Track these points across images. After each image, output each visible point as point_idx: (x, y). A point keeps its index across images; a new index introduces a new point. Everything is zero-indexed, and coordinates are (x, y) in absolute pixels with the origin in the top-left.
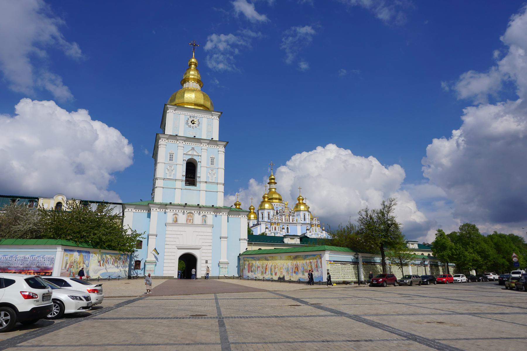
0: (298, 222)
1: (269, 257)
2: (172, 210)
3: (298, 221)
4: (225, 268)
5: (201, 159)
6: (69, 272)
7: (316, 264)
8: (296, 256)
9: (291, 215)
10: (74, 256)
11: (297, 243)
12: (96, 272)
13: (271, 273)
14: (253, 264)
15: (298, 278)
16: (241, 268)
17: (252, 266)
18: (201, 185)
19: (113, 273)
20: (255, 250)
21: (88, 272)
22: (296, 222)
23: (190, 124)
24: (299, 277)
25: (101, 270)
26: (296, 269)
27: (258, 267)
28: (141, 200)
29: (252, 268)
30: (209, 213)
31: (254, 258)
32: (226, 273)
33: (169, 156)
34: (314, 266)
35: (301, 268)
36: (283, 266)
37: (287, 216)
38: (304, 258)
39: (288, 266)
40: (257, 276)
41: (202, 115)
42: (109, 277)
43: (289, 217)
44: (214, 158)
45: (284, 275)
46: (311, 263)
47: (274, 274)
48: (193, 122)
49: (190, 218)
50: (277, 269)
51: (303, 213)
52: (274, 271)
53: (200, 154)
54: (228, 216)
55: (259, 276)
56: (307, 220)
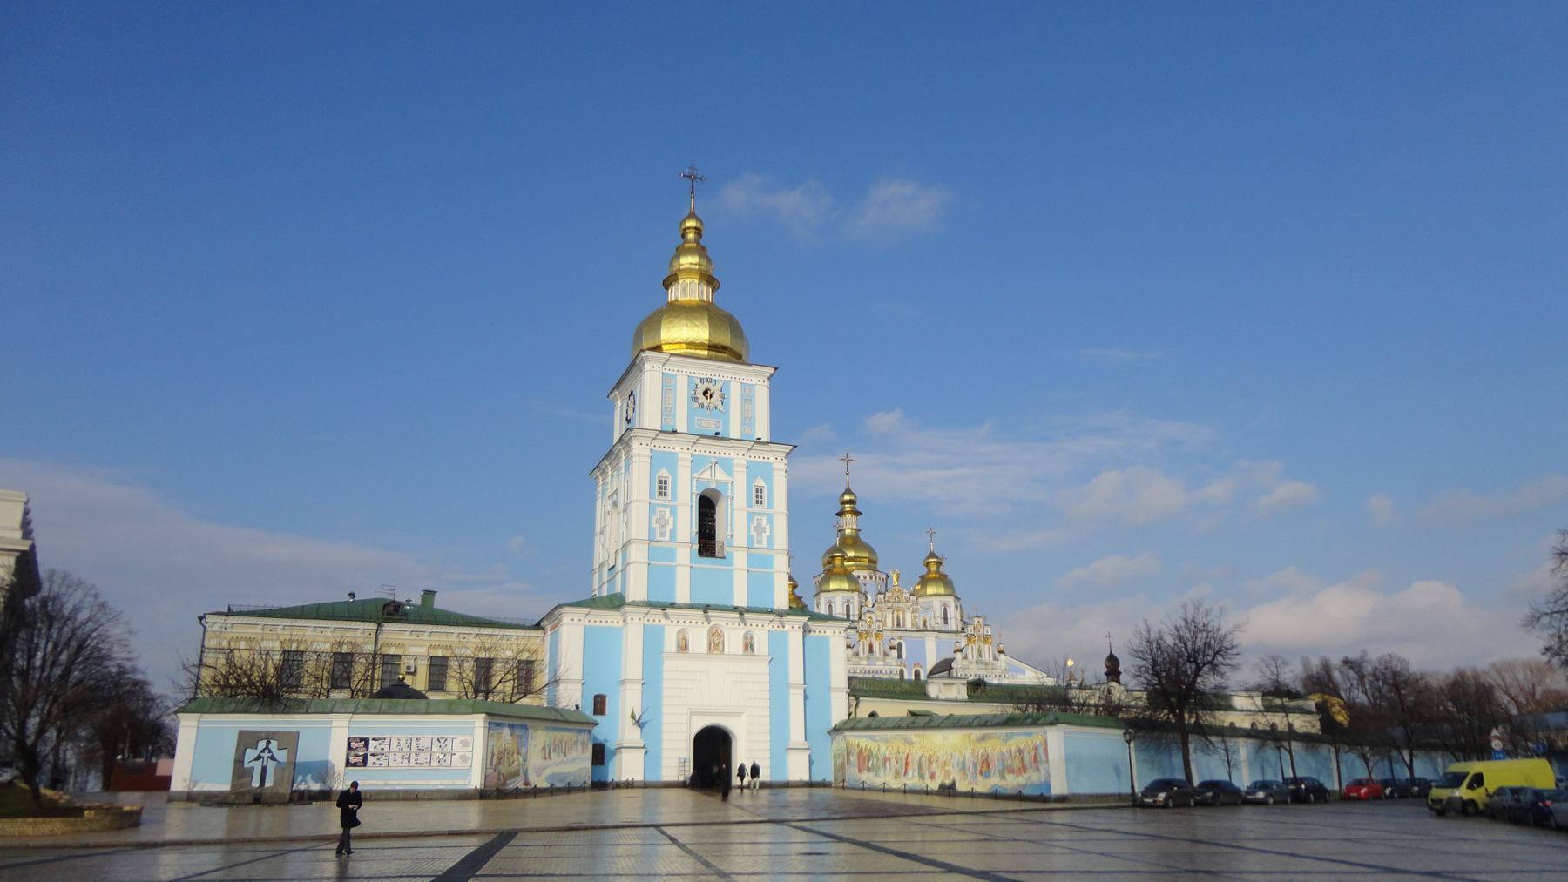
2: (675, 621)
3: (928, 624)
6: (496, 774)
7: (1033, 754)
9: (909, 609)
10: (503, 736)
11: (960, 698)
12: (539, 772)
15: (989, 787)
19: (564, 774)
22: (921, 627)
23: (702, 399)
24: (992, 783)
25: (548, 767)
26: (985, 764)
27: (886, 760)
29: (868, 762)
30: (760, 625)
33: (657, 485)
35: (996, 763)
39: (964, 758)
41: (730, 376)
43: (904, 614)
45: (954, 778)
46: (1020, 751)
47: (927, 776)
49: (716, 640)
52: (929, 768)
53: (731, 479)
56: (953, 621)
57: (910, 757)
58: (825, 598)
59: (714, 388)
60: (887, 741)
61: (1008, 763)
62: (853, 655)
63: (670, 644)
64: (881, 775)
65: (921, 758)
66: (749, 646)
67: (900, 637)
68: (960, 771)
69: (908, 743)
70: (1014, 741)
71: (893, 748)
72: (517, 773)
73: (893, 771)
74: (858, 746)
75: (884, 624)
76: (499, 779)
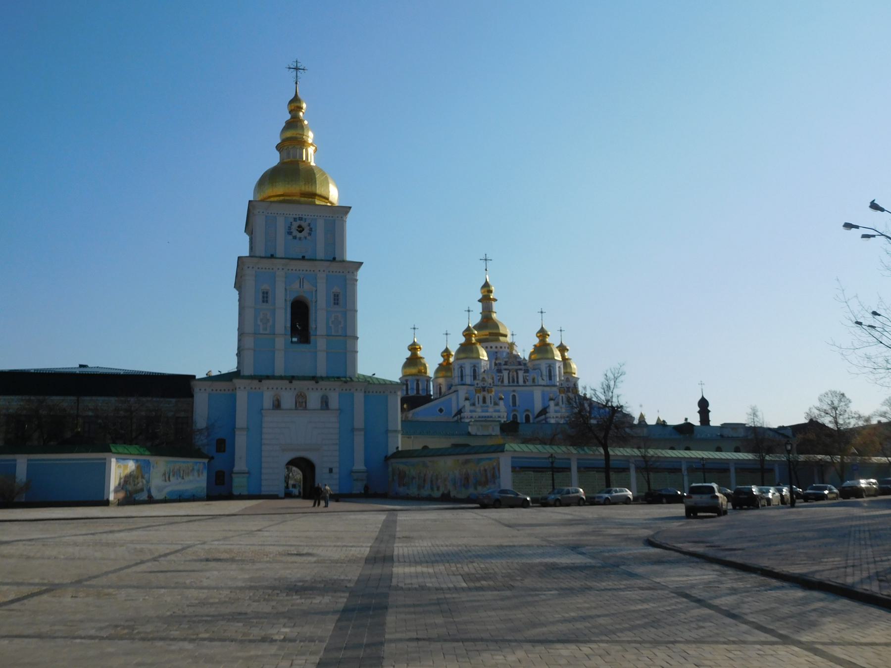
0: (536, 384)
3: (536, 381)
5: (316, 297)
9: (521, 369)
18: (320, 343)
21: (149, 491)
23: (295, 233)
27: (413, 478)
28: (219, 371)
37: (513, 372)
42: (180, 496)
44: (340, 293)
46: (485, 470)
47: (435, 489)
48: (301, 229)
49: (300, 400)
50: (439, 481)
51: (547, 365)
54: (365, 392)
55: (413, 491)
58: (458, 365)
59: (304, 224)
62: (471, 405)
63: (268, 402)
66: (325, 404)
67: (514, 391)
72: (142, 490)
74: (398, 468)
75: (502, 382)
76: (126, 494)
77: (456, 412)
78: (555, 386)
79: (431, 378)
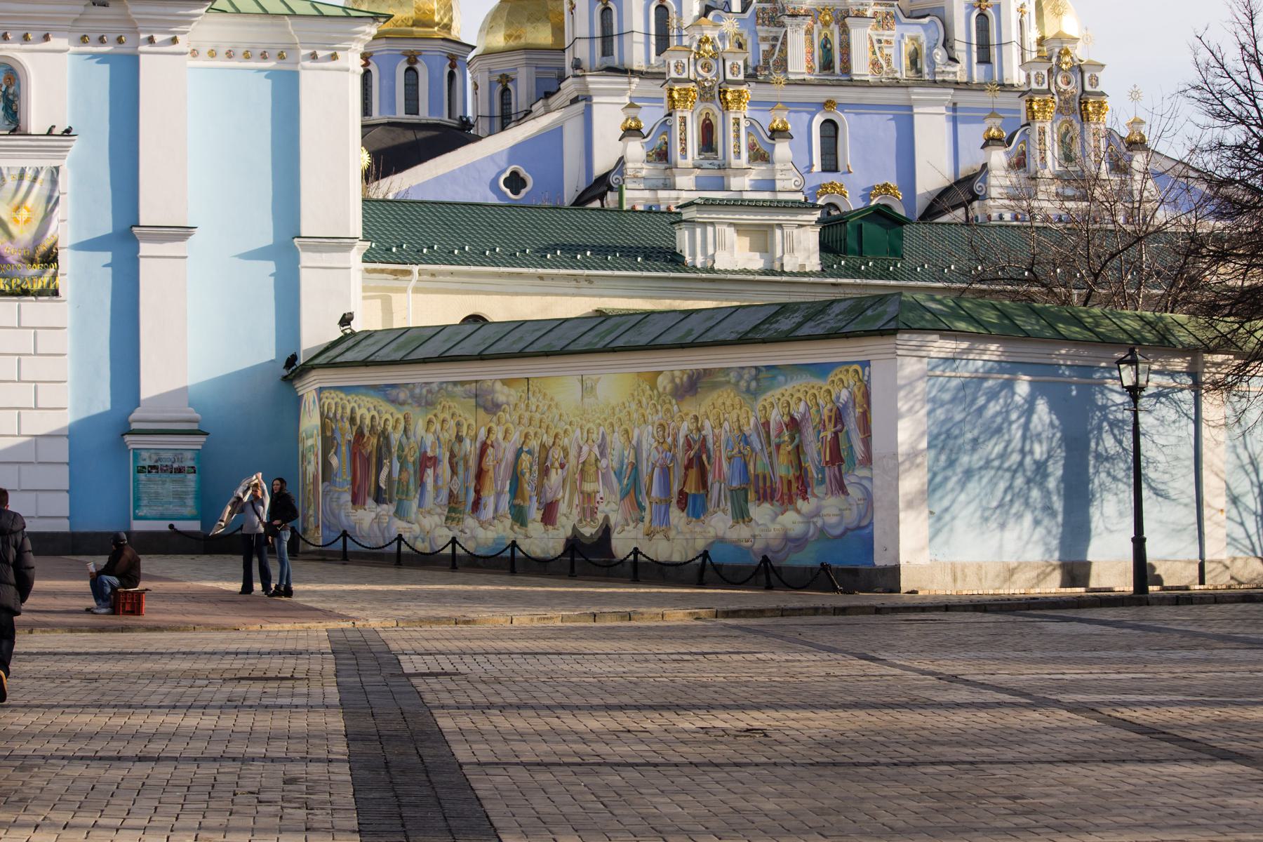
1: (498, 386)
4: (180, 470)
7: (828, 434)
8: (690, 377)
13: (513, 506)
14: (387, 438)
15: (700, 545)
16: (304, 473)
17: (384, 450)
20: (523, 323)
24: (712, 533)
26: (693, 473)
27: (426, 461)
31: (394, 392)
32: (187, 511)
34: (814, 452)
35: (725, 465)
36: (602, 454)
37: (826, 24)
38: (748, 390)
39: (637, 450)
40: (416, 527)
45: (607, 518)
46: (794, 425)
50: (555, 477)
57: (490, 451)
60: (427, 402)
61: (758, 466)
64: (413, 516)
65: (519, 453)
67: (828, 104)
68: (625, 495)
69: (486, 409)
70: (777, 393)
71: (444, 421)
73: (444, 494)
74: (352, 420)
75: (782, 65)
77: (583, 187)
78: (1004, 87)
79: (473, 48)
